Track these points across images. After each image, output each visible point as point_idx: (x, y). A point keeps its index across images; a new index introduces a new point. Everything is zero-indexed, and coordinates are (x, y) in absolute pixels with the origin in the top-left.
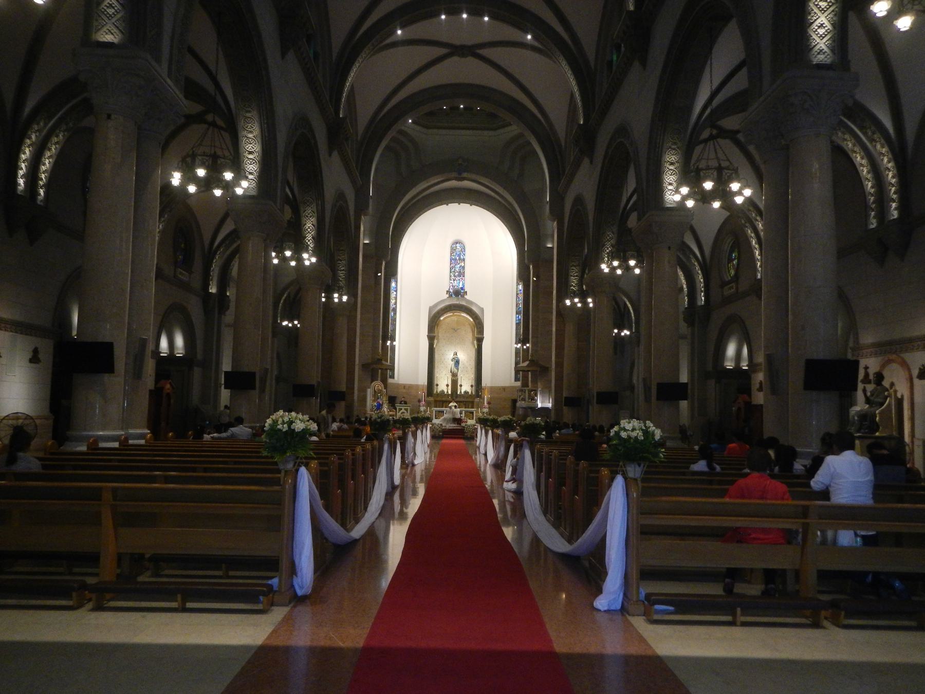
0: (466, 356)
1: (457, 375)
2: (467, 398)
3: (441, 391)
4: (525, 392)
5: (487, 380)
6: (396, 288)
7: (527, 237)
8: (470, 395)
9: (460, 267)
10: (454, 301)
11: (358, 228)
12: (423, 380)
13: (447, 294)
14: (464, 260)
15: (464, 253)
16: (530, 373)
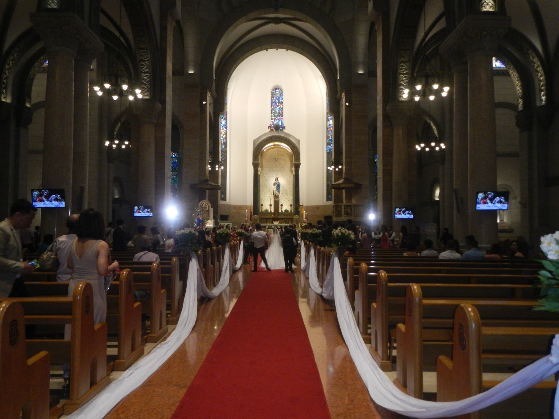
0: (285, 181)
1: (278, 197)
2: (287, 215)
3: (265, 211)
4: (341, 208)
5: (303, 201)
6: (226, 125)
7: (340, 67)
8: (290, 213)
9: (279, 109)
10: (275, 134)
11: (164, 29)
12: (250, 202)
13: (269, 128)
14: (282, 103)
15: (282, 97)
16: (344, 191)
